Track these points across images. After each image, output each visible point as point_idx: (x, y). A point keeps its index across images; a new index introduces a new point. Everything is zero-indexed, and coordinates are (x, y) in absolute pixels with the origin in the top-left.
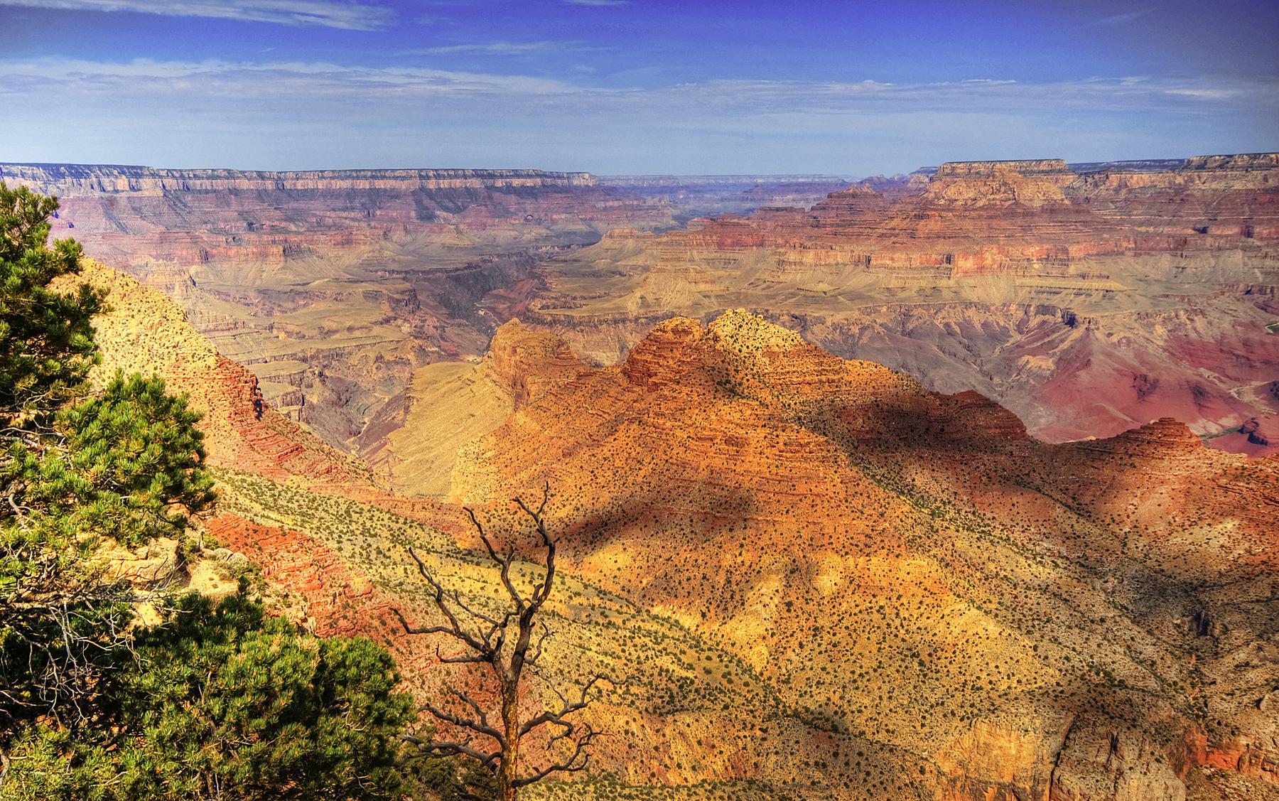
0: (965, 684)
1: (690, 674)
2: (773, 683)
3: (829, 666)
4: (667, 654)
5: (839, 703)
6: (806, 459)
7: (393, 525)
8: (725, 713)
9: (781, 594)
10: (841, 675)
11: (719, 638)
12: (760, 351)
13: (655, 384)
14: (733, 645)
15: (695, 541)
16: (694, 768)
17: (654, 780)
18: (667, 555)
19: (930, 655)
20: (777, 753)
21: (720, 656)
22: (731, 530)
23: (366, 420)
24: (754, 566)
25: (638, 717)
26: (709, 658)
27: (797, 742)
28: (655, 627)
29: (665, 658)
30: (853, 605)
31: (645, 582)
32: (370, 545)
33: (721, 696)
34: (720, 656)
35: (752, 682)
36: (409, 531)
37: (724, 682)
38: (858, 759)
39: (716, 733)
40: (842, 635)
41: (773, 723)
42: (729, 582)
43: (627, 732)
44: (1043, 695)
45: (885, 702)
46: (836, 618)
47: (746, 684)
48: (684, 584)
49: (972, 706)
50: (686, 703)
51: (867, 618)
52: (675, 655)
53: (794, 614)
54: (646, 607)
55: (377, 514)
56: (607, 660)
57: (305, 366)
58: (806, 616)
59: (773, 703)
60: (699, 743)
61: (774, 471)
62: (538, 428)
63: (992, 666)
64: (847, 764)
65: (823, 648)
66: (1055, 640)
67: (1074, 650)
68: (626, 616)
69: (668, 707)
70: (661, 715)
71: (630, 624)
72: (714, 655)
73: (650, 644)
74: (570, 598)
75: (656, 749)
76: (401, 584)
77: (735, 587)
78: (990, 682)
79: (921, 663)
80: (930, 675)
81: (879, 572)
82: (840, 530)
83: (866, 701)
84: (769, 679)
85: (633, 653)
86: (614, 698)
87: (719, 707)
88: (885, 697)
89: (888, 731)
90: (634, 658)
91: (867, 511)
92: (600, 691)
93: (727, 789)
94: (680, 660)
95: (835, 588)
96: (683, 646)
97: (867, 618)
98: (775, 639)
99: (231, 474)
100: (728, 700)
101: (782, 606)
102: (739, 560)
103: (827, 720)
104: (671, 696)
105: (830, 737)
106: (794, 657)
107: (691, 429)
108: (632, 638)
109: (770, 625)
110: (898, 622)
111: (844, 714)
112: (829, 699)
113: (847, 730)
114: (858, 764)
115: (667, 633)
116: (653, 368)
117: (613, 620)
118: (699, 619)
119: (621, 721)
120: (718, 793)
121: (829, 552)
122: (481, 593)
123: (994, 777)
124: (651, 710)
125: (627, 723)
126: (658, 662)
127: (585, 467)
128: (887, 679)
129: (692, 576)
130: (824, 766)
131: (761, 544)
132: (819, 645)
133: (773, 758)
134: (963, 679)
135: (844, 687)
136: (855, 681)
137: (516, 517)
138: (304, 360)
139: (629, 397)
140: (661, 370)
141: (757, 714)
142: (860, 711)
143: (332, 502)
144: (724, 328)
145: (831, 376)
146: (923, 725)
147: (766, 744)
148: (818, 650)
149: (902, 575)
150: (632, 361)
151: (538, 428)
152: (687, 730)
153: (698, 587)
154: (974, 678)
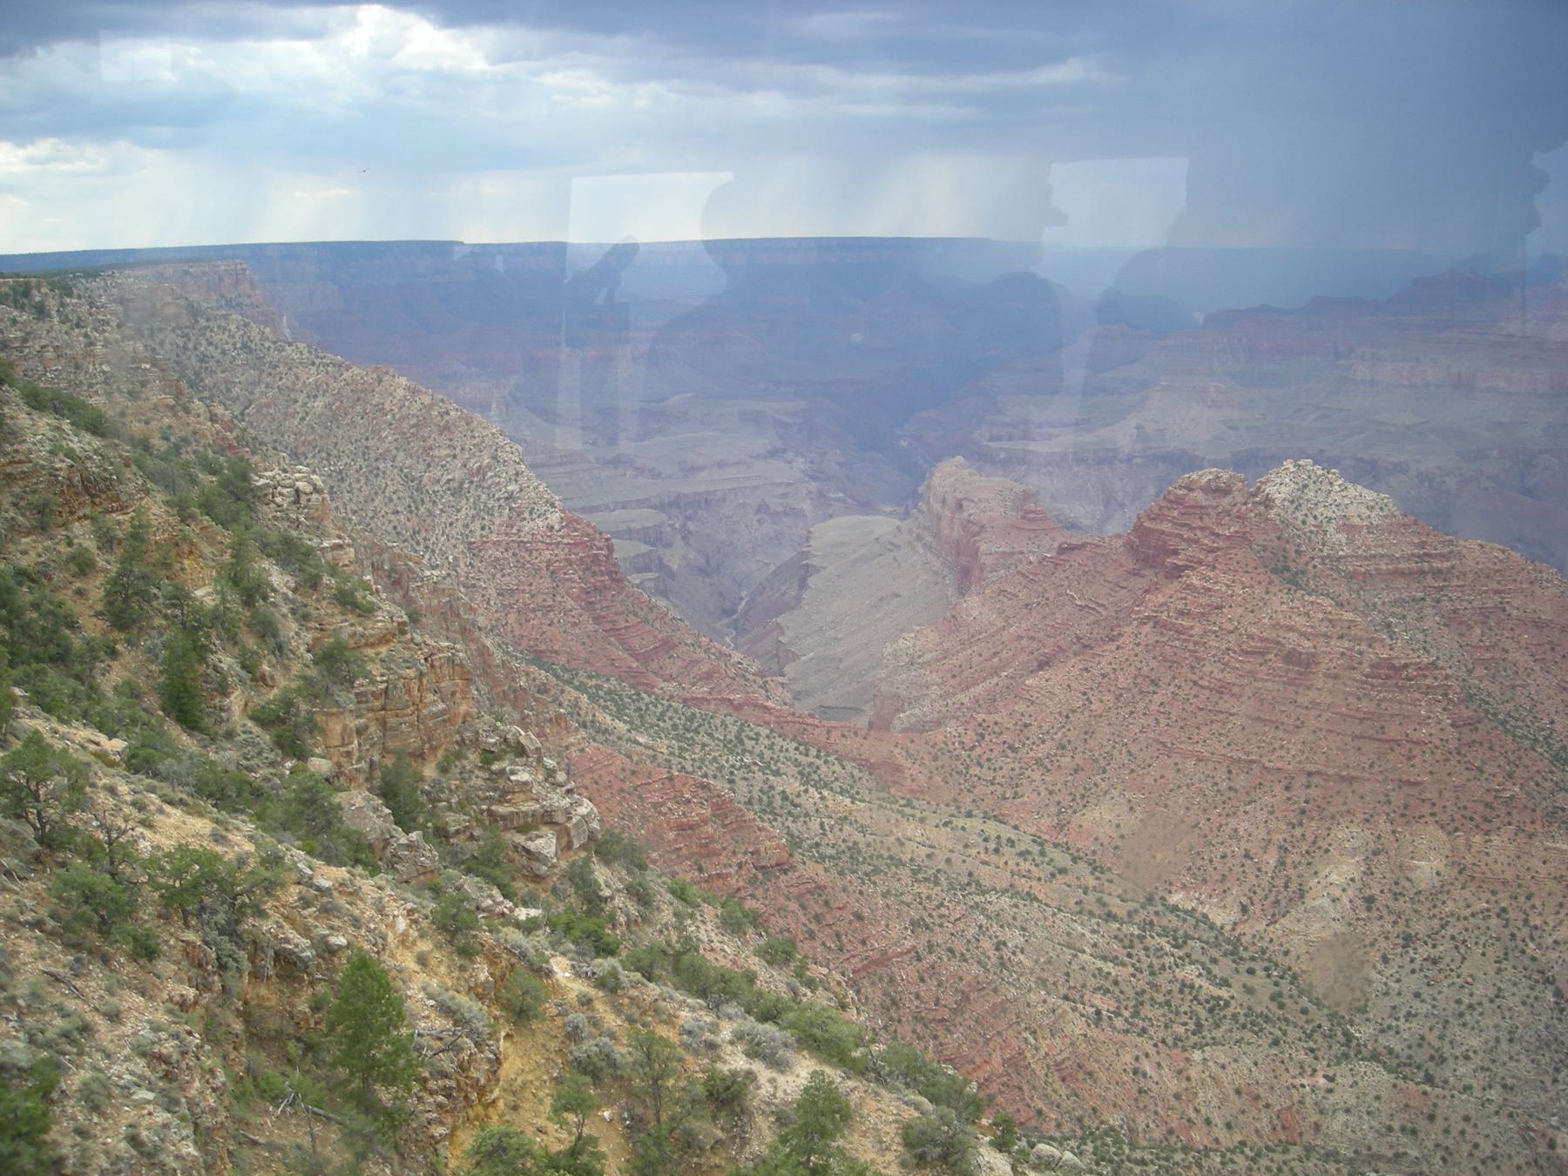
1: (1224, 993)
3: (1426, 992)
4: (1192, 963)
5: (1436, 1043)
6: (1401, 689)
7: (801, 758)
8: (1274, 1051)
9: (1359, 884)
10: (1441, 1004)
11: (1265, 945)
12: (1333, 525)
13: (1176, 567)
14: (1286, 953)
15: (1235, 802)
16: (1228, 1126)
17: (1173, 1139)
18: (1193, 820)
20: (1348, 1111)
21: (1266, 969)
22: (1287, 788)
23: (744, 593)
24: (1320, 843)
25: (1152, 1051)
26: (1251, 972)
27: (1378, 1098)
30: (1462, 904)
31: (1159, 856)
32: (772, 788)
33: (1268, 1027)
34: (1266, 969)
35: (1312, 1008)
36: (824, 768)
37: (1273, 1006)
38: (1462, 1125)
39: (1262, 1078)
40: (1444, 947)
45: (1504, 1046)
46: (1436, 923)
47: (1304, 1011)
50: (1218, 1034)
51: (1483, 924)
52: (1203, 964)
53: (1376, 914)
55: (779, 741)
56: (1108, 967)
57: (664, 516)
58: (1394, 918)
59: (1341, 1039)
60: (1238, 1092)
61: (1352, 700)
62: (1000, 624)
64: (1447, 1131)
65: (1416, 966)
68: (1131, 905)
69: (1194, 1039)
70: (1184, 1050)
71: (1141, 916)
72: (1258, 967)
73: (1168, 948)
74: (1053, 875)
75: (1177, 1096)
76: (817, 845)
77: (1291, 872)
81: (1502, 858)
82: (1447, 794)
83: (1475, 1042)
84: (1338, 1004)
85: (1143, 958)
86: (1119, 1022)
87: (1265, 1042)
88: (1504, 1036)
90: (1144, 966)
91: (1490, 769)
92: (1098, 1013)
93: (1278, 1157)
94: (1209, 972)
95: (1436, 882)
96: (1214, 953)
97: (1483, 924)
99: (582, 676)
102: (1298, 832)
104: (1199, 1025)
105: (1425, 1093)
106: (1374, 975)
107: (1231, 638)
108: (1141, 938)
109: (1339, 927)
110: (1525, 932)
111: (1443, 1060)
112: (1423, 1038)
113: (1446, 1082)
114: (1463, 1132)
116: (1173, 543)
117: (1114, 910)
118: (1233, 915)
119: (1128, 1058)
120: (1264, 1162)
121: (1432, 828)
122: (927, 862)
124: (1170, 1041)
125: (1137, 1059)
126: (1179, 973)
127: (1073, 685)
128: (1507, 1014)
129: (1228, 851)
130: (1414, 1132)
131: (1333, 810)
132: (1412, 960)
133: (1342, 1117)
136: (1461, 1015)
137: (974, 754)
138: (661, 507)
139: (1139, 584)
140: (1184, 545)
141: (1320, 1054)
142: (1467, 1058)
143: (718, 722)
144: (1280, 486)
145: (1437, 564)
146: (1555, 1081)
147: (1332, 1098)
148: (1409, 967)
149: (1536, 863)
150: (1139, 530)
151: (1000, 624)
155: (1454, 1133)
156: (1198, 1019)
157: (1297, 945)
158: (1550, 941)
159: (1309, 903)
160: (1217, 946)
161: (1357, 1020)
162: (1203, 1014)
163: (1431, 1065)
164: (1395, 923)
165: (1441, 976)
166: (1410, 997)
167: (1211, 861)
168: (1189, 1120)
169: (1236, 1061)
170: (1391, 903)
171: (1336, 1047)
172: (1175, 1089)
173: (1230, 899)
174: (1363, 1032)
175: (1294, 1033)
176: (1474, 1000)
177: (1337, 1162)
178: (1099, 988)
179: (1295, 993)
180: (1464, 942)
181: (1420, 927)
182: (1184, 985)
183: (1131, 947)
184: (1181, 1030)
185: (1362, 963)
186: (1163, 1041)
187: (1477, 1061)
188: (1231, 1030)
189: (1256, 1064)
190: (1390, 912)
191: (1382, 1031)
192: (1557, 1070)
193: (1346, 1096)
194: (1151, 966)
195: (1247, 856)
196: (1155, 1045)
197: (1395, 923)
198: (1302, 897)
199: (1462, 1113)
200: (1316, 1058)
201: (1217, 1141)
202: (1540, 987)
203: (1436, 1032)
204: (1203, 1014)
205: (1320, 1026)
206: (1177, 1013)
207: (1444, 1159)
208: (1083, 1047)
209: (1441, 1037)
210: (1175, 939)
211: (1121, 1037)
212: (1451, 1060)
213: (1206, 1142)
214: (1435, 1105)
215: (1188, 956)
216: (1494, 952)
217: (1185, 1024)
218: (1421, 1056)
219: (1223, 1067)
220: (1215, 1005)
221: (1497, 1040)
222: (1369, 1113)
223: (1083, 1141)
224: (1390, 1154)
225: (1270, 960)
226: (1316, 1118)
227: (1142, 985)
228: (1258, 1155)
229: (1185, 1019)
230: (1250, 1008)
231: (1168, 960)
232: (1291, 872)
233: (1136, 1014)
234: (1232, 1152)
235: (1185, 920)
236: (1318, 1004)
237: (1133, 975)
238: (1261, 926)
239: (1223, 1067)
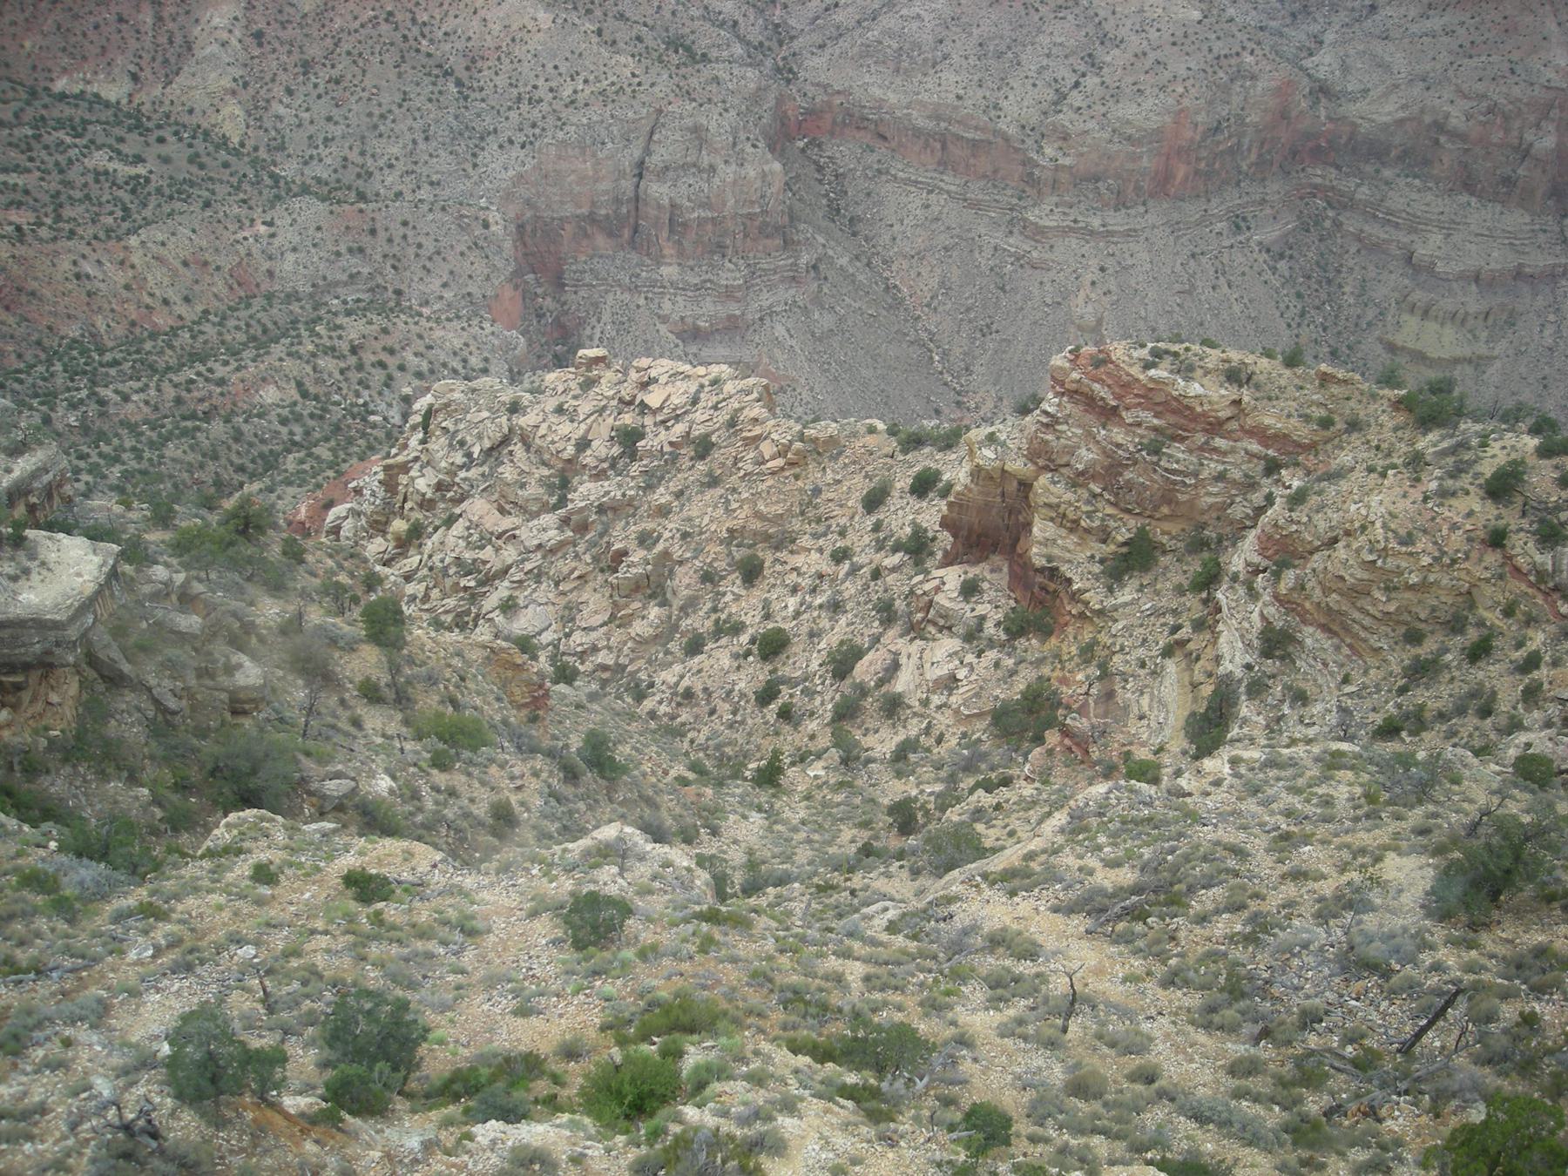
0: (519, 99)
1: (141, 170)
2: (262, 154)
3: (335, 112)
4: (99, 148)
5: (360, 160)
8: (208, 213)
9: (243, 22)
10: (354, 121)
11: (166, 108)
14: (191, 111)
16: (187, 300)
17: (137, 331)
19: (468, 68)
20: (294, 250)
21: (176, 133)
25: (87, 250)
26: (161, 140)
27: (319, 228)
28: (68, 111)
29: (97, 154)
30: (350, 17)
31: (28, 44)
33: (196, 191)
37: (194, 169)
38: (402, 230)
39: (204, 243)
40: (343, 64)
41: (280, 208)
42: (160, 19)
43: (78, 276)
44: (617, 93)
45: (422, 146)
46: (329, 42)
47: (226, 165)
48: (91, 34)
49: (534, 126)
50: (147, 213)
51: (374, 33)
52: (110, 147)
54: (43, 84)
58: (287, 47)
59: (268, 181)
60: (185, 264)
63: (550, 66)
64: (390, 240)
65: (321, 89)
66: (621, 16)
67: (645, 25)
68: (15, 106)
69: (126, 225)
70: (119, 239)
71: (30, 113)
72: (166, 133)
73: (68, 140)
75: (127, 287)
77: (171, 25)
78: (551, 90)
79: (459, 83)
80: (473, 96)
83: (395, 150)
84: (256, 149)
85: (47, 158)
86: (44, 232)
87: (196, 206)
88: (420, 137)
89: (432, 184)
90: (50, 166)
92: (19, 229)
93: (243, 314)
94: (119, 153)
96: (118, 131)
97: (374, 33)
98: (251, 91)
100: (207, 194)
101: (249, 40)
103: (349, 188)
104: (125, 209)
105: (361, 211)
106: (282, 110)
108: (37, 137)
109: (238, 72)
110: (416, 30)
111: (370, 174)
112: (345, 159)
113: (377, 195)
114: (405, 237)
115: (87, 116)
119: (65, 265)
120: (231, 323)
123: (569, 210)
124: (102, 235)
125: (75, 263)
128: (417, 115)
129: (99, 19)
130: (361, 250)
132: (316, 86)
133: (291, 257)
134: (515, 92)
135: (363, 137)
136: (375, 127)
141: (252, 203)
142: (391, 166)
146: (475, 166)
147: (276, 242)
152: (162, 251)
153: (115, 37)
154: (529, 88)
155: (397, 240)
156: (124, 204)
157: (199, 99)
158: (440, 34)
159: (199, 54)
160: (119, 123)
161: (279, 160)
162: (127, 197)
163: (360, 182)
164: (290, 52)
165: (347, 94)
166: (323, 122)
167: (85, 35)
168: (147, 307)
169: (173, 234)
170: (280, 34)
171: (266, 191)
172: (123, 282)
173: (116, 71)
174: (288, 169)
175: (222, 190)
176: (384, 109)
177: (299, 300)
178: (12, 203)
179: (211, 149)
180: (360, 55)
181: (314, 51)
182: (97, 173)
183: (30, 149)
184: (110, 220)
185: (268, 101)
186: (96, 237)
187: (400, 166)
188: (159, 205)
189: (194, 231)
190: (282, 44)
191: (306, 163)
192: (474, 155)
193: (289, 236)
194: (57, 164)
195: (121, 20)
196: (89, 244)
197: (290, 52)
198: (190, 49)
199: (399, 219)
200: (250, 208)
201: (180, 317)
202: (441, 81)
203: (356, 150)
204: (127, 197)
205: (245, 175)
206: (100, 205)
207: (394, 267)
208: (15, 269)
209: (363, 153)
210: (73, 129)
211: (51, 247)
212: (377, 173)
213: (170, 322)
214: (373, 219)
215: (92, 142)
216: (391, 58)
217: (111, 213)
218: (349, 176)
219: (163, 244)
220: (136, 185)
221: (414, 142)
222: (315, 245)
223: (49, 362)
224: (345, 278)
225: (177, 123)
226: (267, 265)
227: (54, 187)
228: (224, 318)
229: (110, 207)
230: (171, 178)
231: (73, 153)
232: (171, 25)
233: (58, 218)
234: (198, 323)
235: (77, 106)
236: (236, 153)
237: (42, 179)
238: (157, 91)
239: (163, 244)
